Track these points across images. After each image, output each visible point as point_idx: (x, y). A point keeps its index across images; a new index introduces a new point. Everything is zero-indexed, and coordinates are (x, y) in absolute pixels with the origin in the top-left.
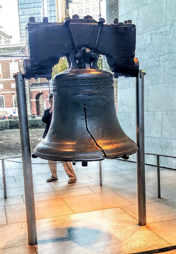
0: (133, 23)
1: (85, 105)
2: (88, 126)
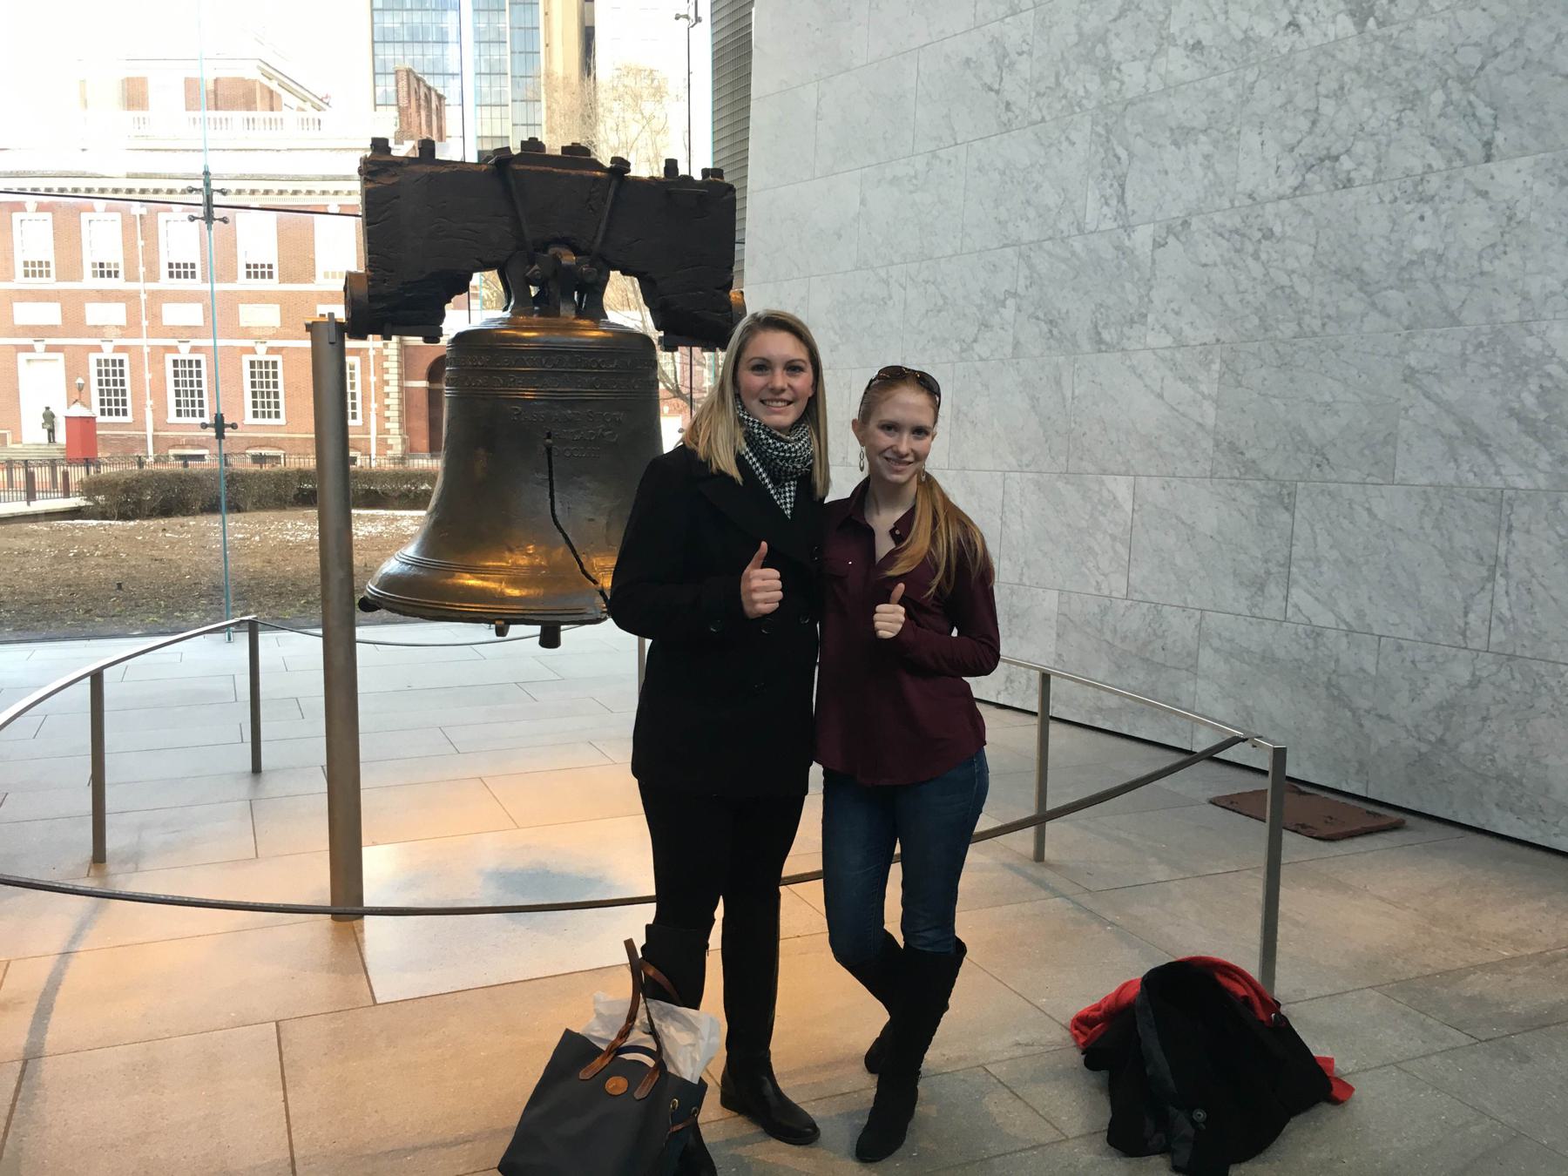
0: (727, 179)
1: (549, 436)
2: (558, 506)
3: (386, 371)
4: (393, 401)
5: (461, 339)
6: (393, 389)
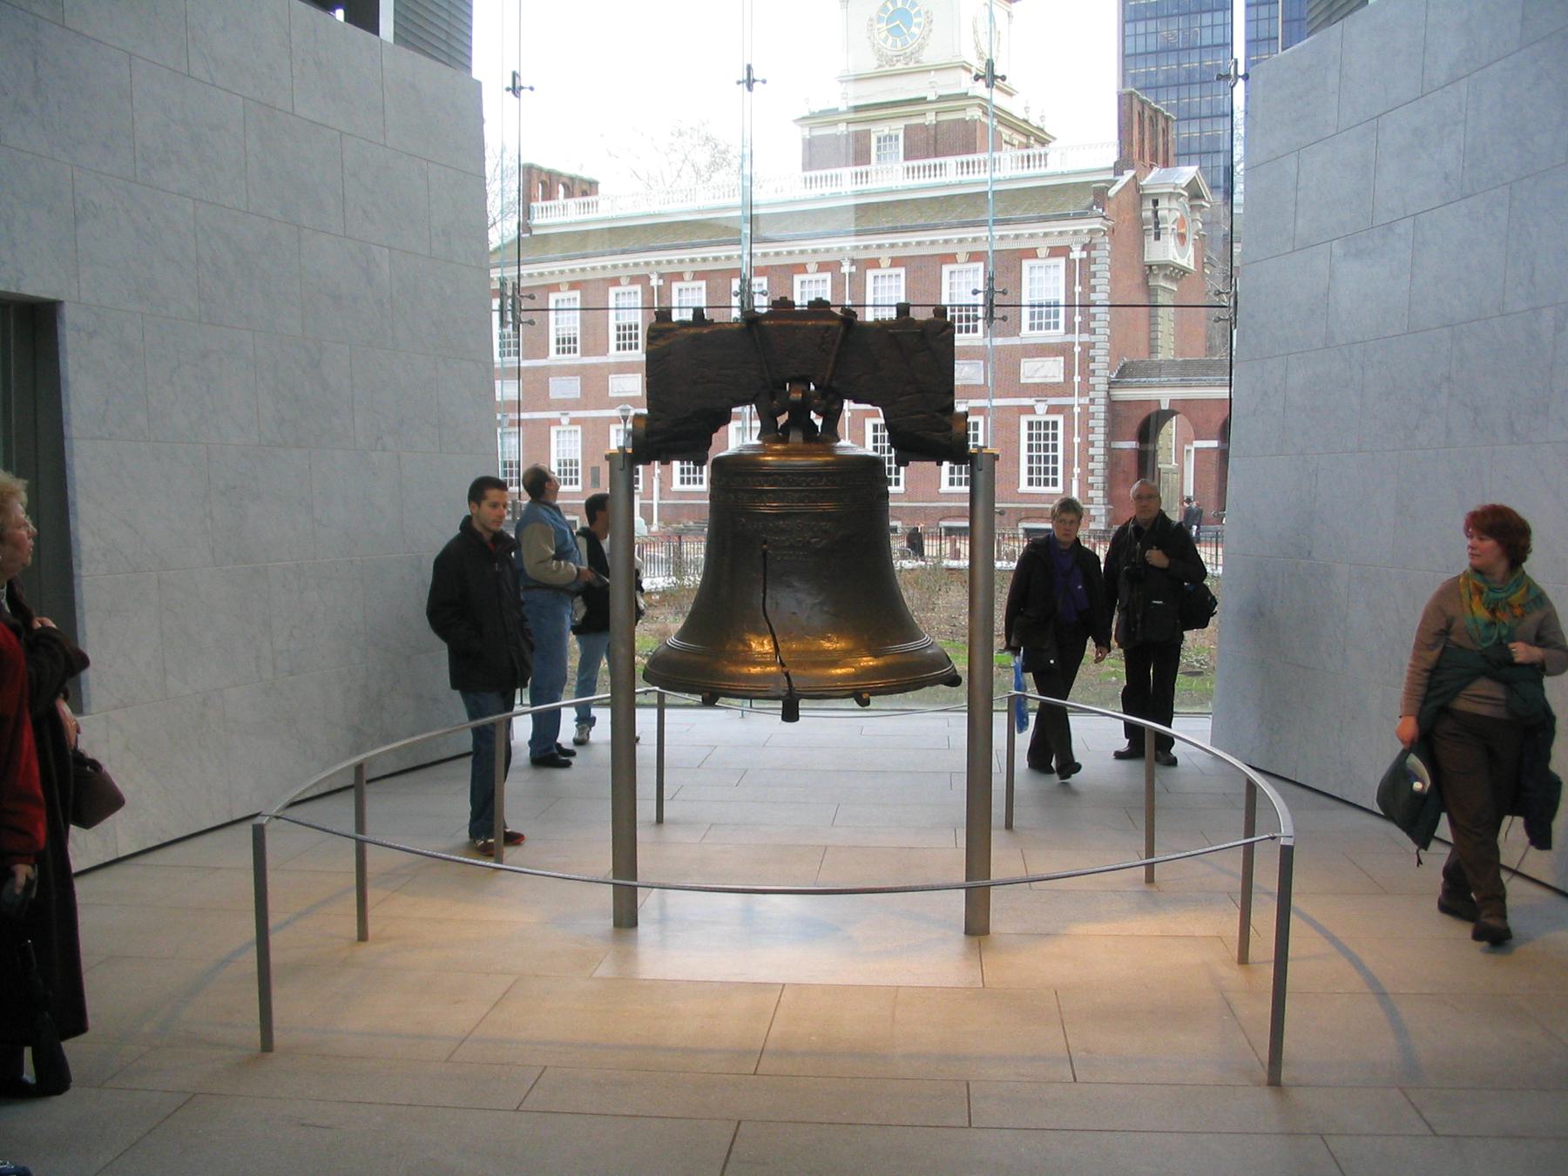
2: (768, 601)
3: (1092, 430)
4: (1098, 466)
5: (719, 464)
6: (1098, 451)
